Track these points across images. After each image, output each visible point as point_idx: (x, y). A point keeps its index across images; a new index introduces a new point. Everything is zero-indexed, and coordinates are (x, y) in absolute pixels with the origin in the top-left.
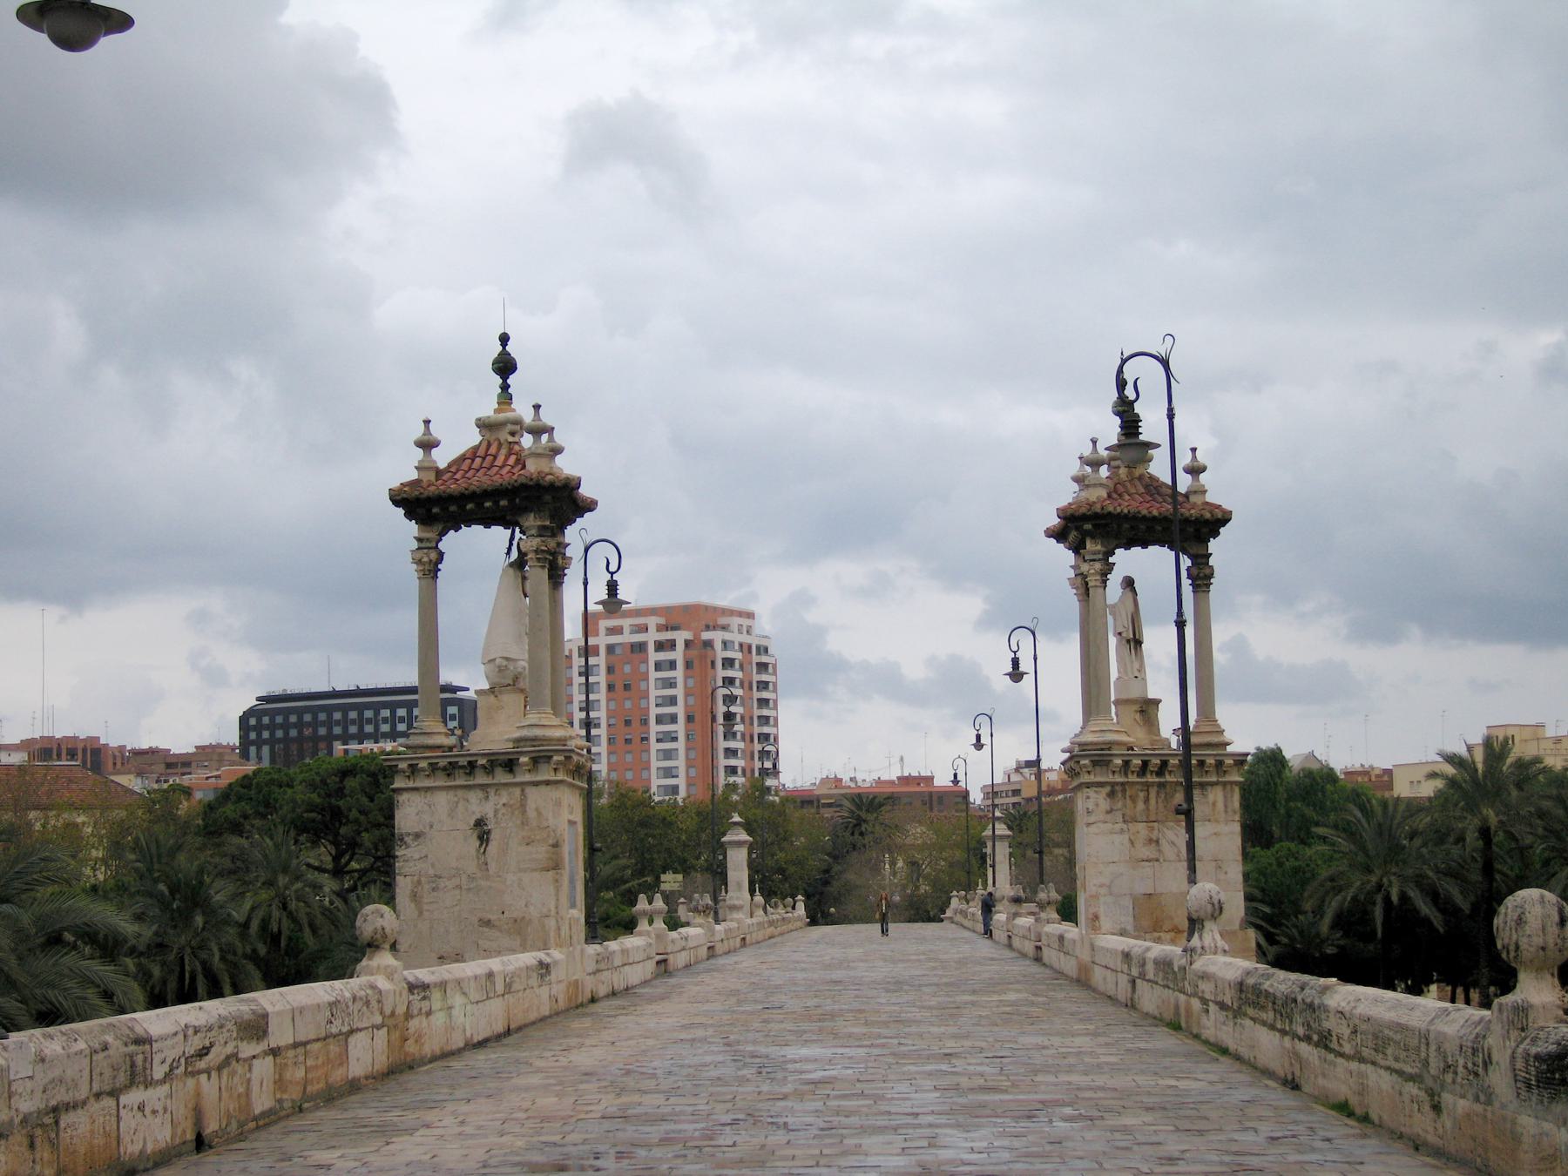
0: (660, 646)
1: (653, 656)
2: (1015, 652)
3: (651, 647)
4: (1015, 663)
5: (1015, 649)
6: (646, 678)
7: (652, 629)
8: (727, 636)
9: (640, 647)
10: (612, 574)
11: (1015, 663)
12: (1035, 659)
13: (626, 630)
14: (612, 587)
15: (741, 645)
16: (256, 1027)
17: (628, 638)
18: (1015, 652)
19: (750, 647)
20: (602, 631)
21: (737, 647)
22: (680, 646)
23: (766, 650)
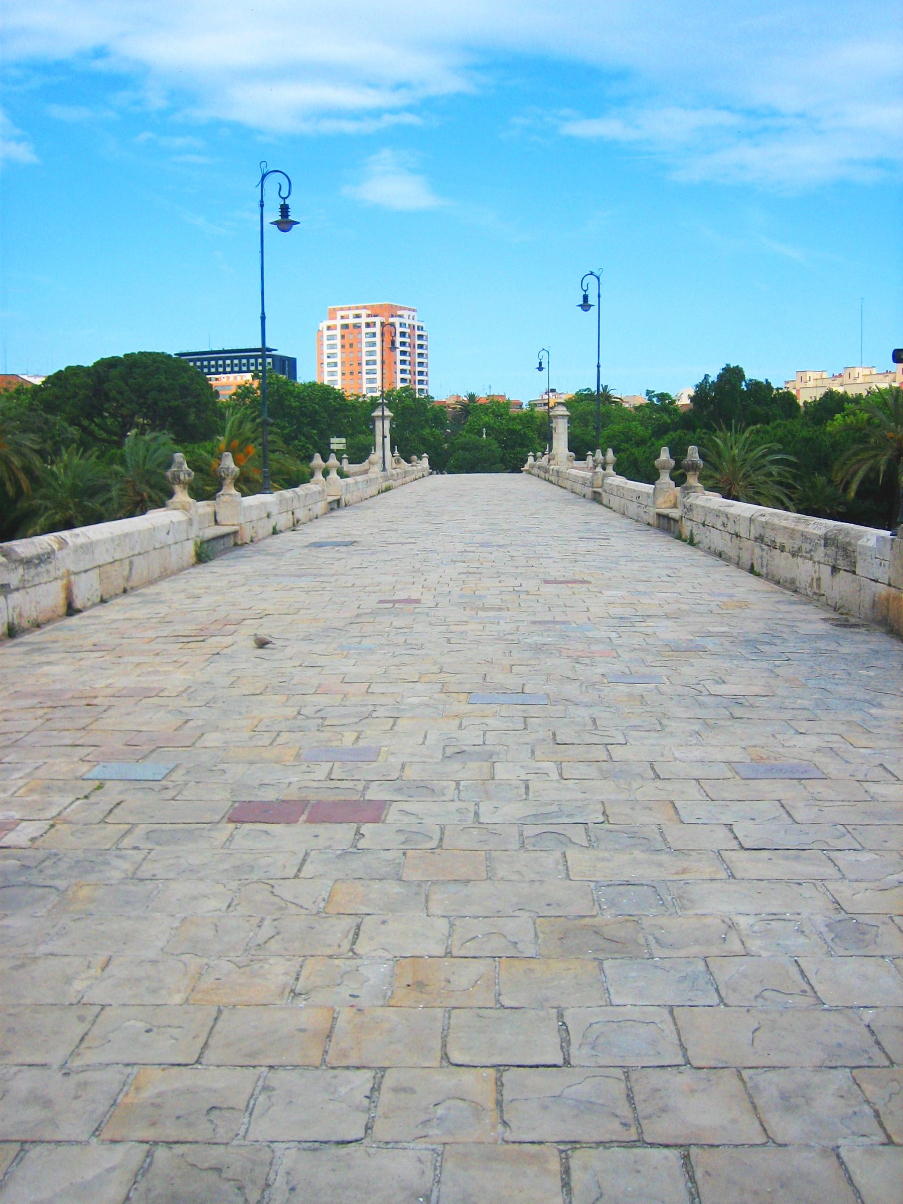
0: (368, 325)
1: (365, 330)
2: (585, 291)
3: (363, 326)
4: (585, 298)
5: (585, 288)
6: (360, 342)
7: (364, 316)
8: (402, 320)
9: (357, 326)
10: (284, 199)
11: (585, 298)
12: (599, 296)
13: (351, 317)
14: (285, 209)
15: (409, 325)
16: (63, 543)
17: (351, 321)
18: (585, 291)
19: (414, 326)
20: (339, 317)
21: (407, 326)
22: (378, 325)
23: (422, 328)
